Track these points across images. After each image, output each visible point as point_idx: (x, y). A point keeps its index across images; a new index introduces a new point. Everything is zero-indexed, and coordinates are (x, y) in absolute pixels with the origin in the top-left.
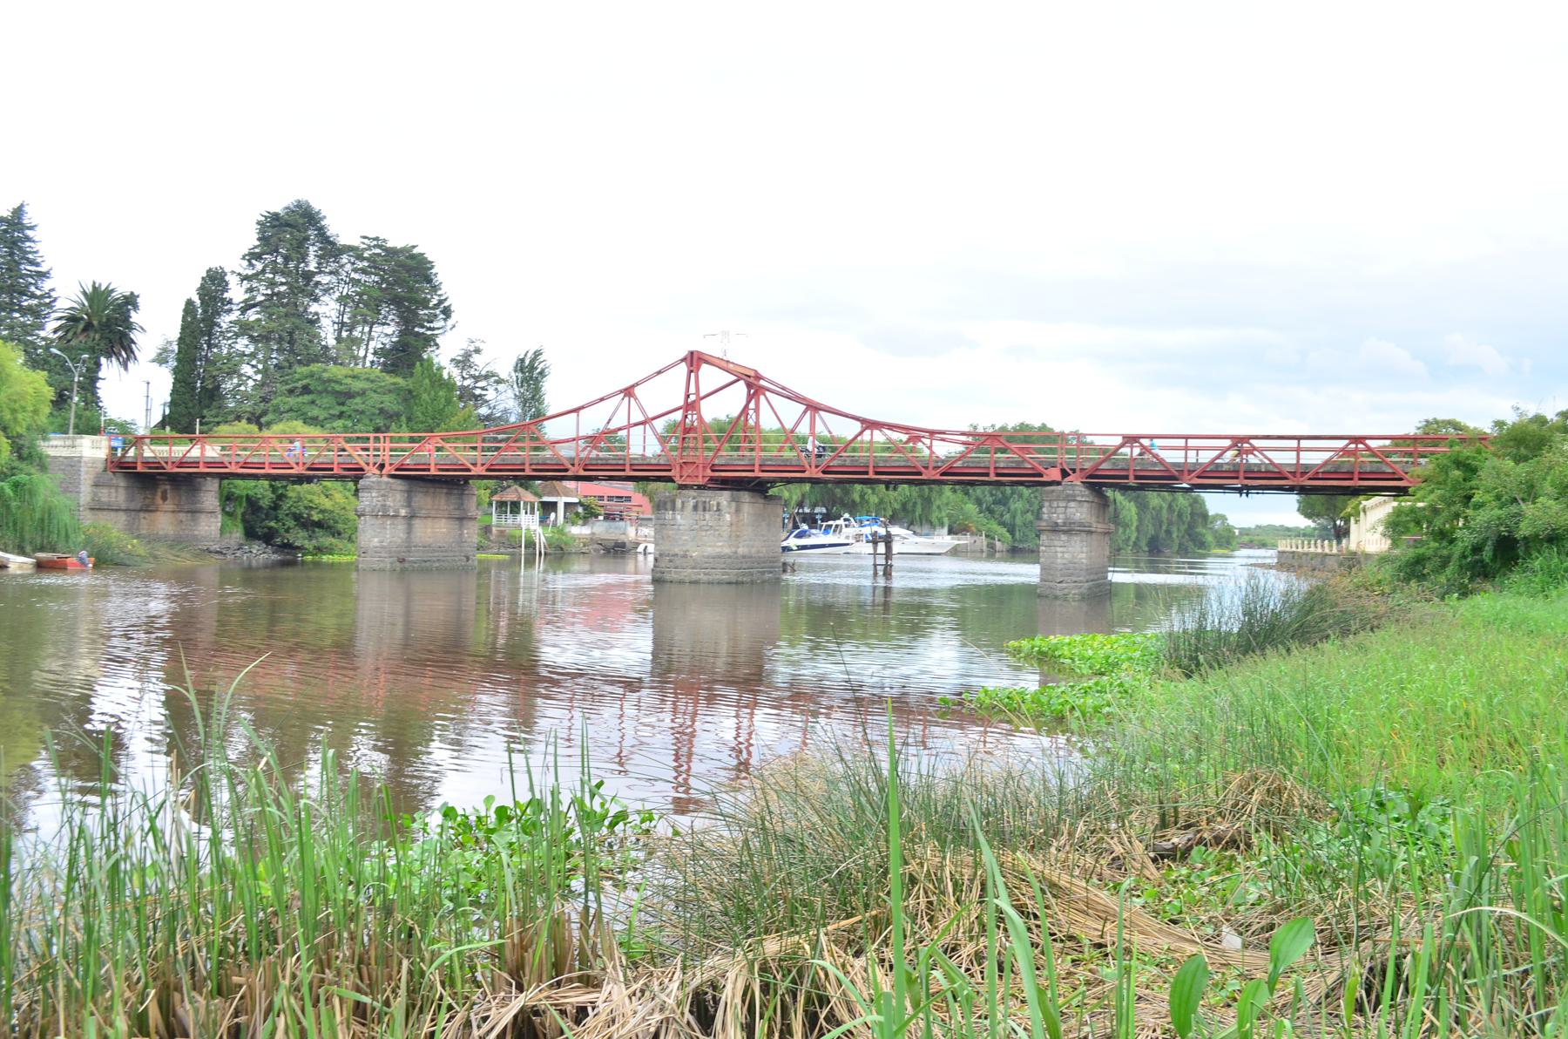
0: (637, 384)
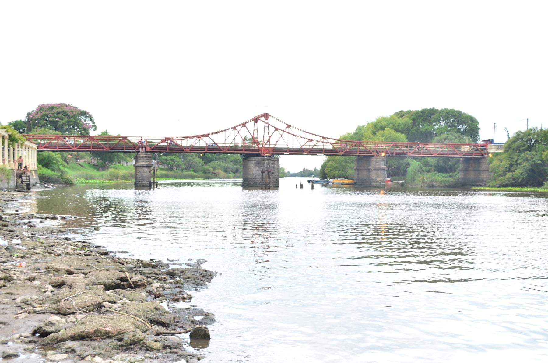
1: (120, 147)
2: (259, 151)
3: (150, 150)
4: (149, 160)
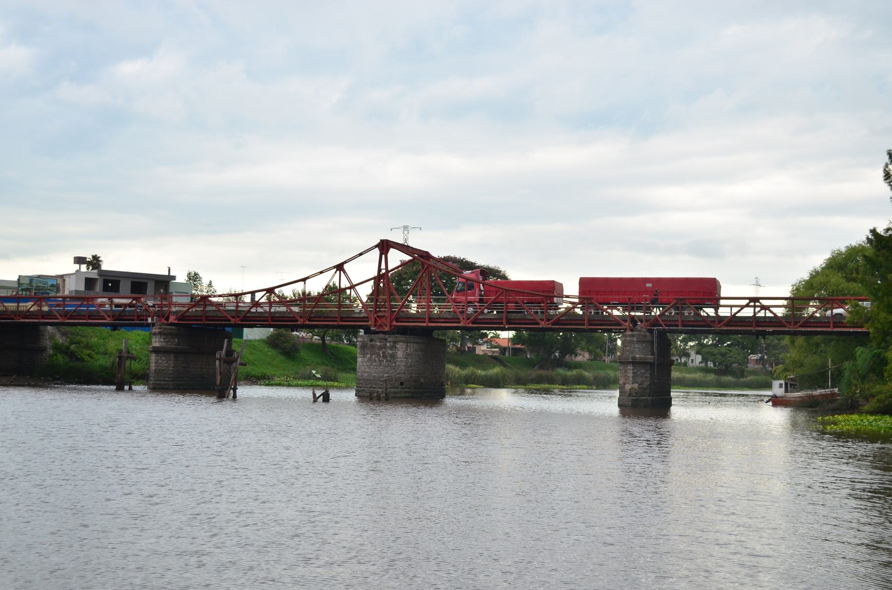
0: (345, 262)
1: (130, 316)
2: (368, 321)
3: (175, 319)
4: (166, 340)
